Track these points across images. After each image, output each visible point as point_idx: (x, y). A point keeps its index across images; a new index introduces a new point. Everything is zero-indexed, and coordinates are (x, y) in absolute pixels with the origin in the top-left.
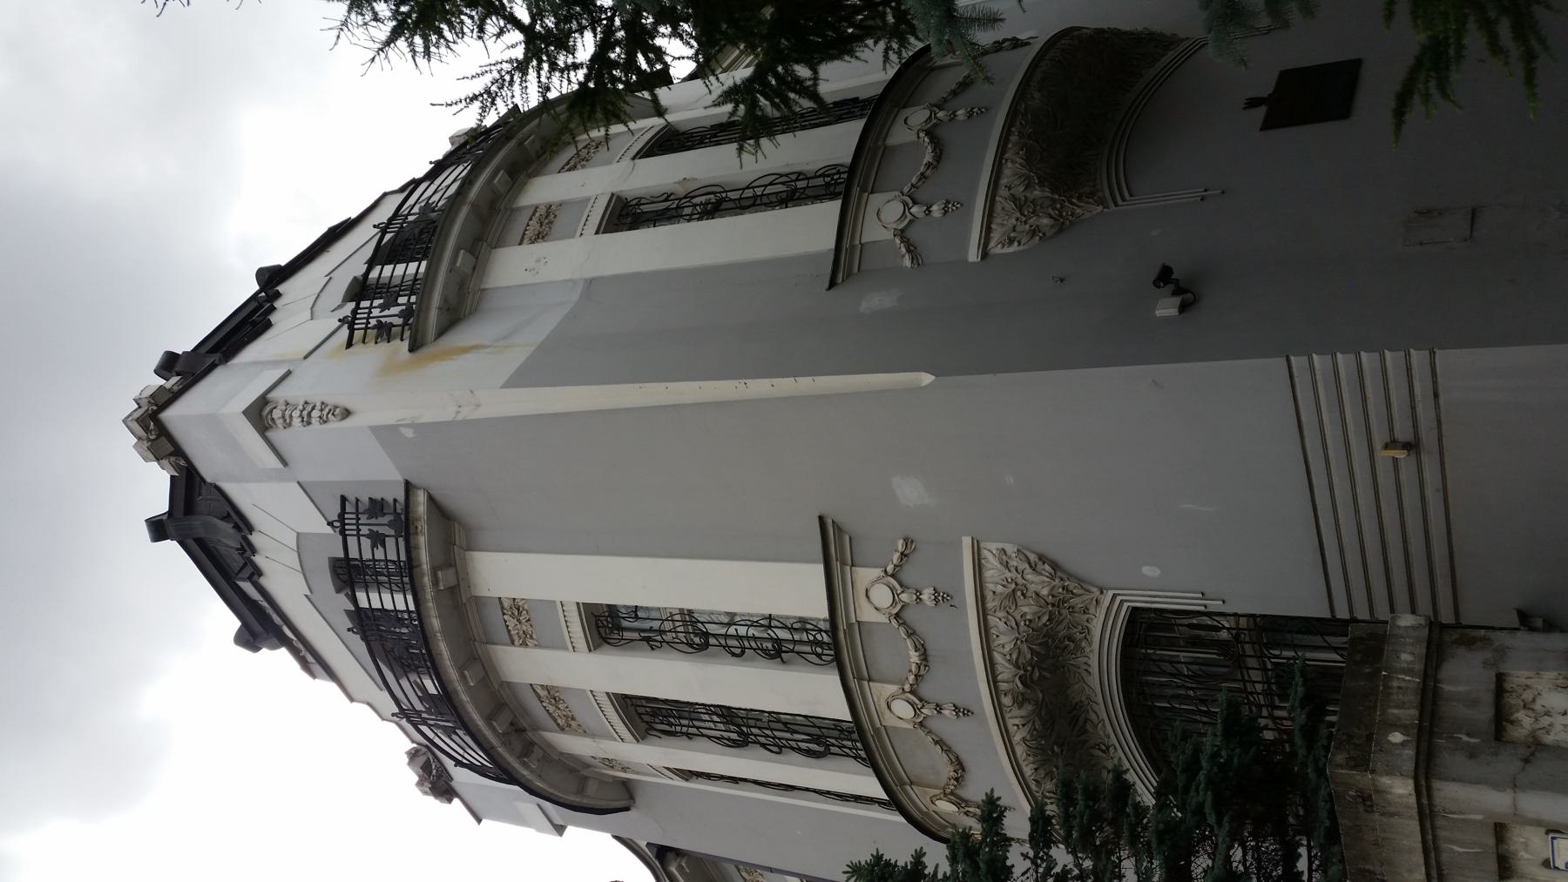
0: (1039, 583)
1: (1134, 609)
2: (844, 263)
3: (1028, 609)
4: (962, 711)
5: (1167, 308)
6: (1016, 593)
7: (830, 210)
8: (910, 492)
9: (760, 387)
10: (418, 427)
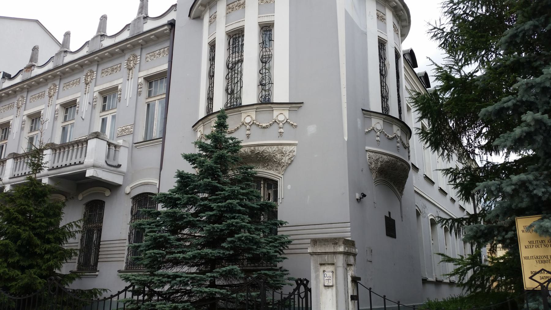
0: (285, 160)
1: (277, 182)
2: (367, 113)
3: (279, 156)
4: (248, 136)
5: (358, 196)
8: (312, 129)
9: (344, 92)
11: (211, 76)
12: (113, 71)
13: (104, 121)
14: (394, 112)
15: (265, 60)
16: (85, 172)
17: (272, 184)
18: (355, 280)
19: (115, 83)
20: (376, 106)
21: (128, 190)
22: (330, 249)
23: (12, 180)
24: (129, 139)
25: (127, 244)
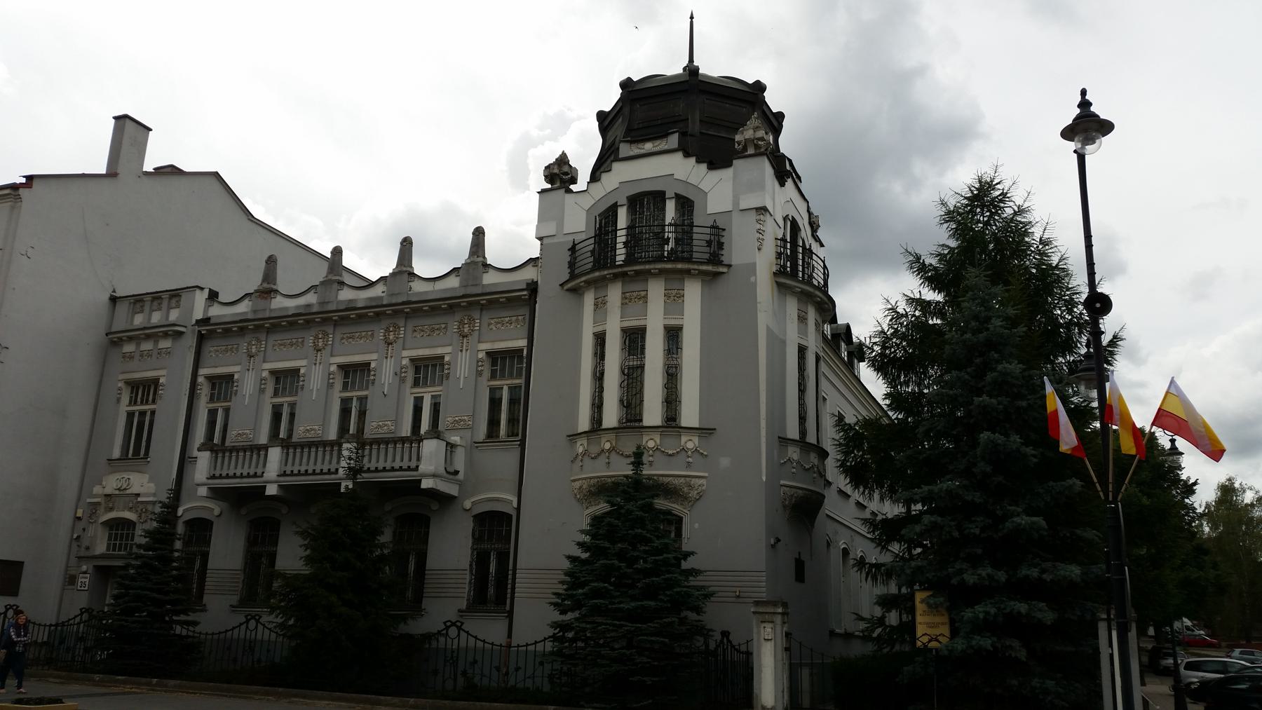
0: (694, 494)
1: (681, 519)
2: (784, 441)
5: (772, 541)
7: (797, 437)
8: (725, 462)
9: (763, 424)
10: (755, 284)
11: (599, 377)
12: (433, 330)
14: (811, 439)
18: (788, 635)
19: (439, 351)
20: (793, 432)
21: (468, 504)
23: (282, 479)
24: (468, 434)
25: (468, 577)
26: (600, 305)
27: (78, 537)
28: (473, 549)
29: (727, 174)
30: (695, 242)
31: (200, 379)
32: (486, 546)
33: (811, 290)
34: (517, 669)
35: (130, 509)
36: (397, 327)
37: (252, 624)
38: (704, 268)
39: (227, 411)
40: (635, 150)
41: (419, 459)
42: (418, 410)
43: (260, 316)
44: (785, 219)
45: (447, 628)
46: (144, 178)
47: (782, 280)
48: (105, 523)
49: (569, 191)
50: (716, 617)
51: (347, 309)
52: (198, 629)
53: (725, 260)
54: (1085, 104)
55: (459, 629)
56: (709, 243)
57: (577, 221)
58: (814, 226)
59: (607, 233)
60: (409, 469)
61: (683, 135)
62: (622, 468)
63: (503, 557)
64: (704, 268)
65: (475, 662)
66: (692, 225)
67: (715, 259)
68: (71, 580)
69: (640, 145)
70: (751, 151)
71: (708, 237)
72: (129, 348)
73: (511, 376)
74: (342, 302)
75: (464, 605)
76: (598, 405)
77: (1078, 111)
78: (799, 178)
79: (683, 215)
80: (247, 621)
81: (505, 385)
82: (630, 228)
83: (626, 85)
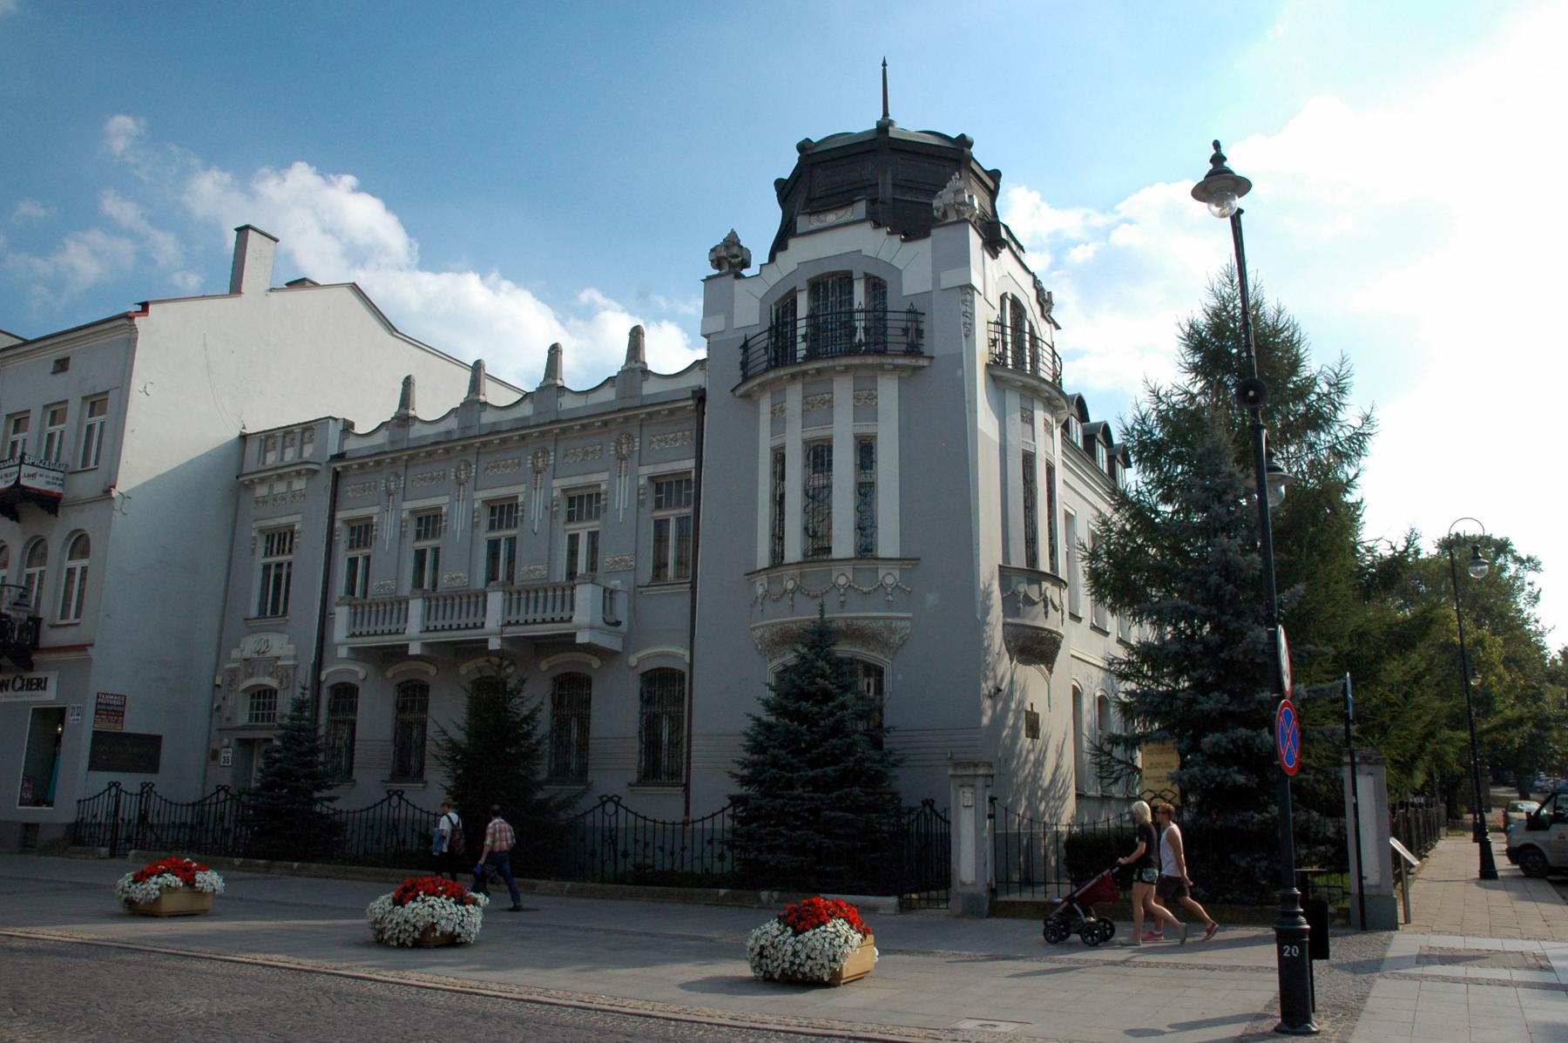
0: (896, 639)
6: (892, 631)
11: (779, 501)
12: (586, 453)
13: (574, 539)
15: (865, 491)
16: (574, 635)
17: (876, 672)
18: (992, 800)
19: (594, 478)
21: (633, 661)
22: (971, 772)
26: (778, 414)
27: (219, 707)
28: (642, 714)
29: (923, 247)
30: (890, 331)
31: (338, 524)
32: (657, 709)
33: (1036, 383)
34: (683, 849)
35: (271, 675)
36: (546, 452)
37: (395, 799)
38: (900, 361)
39: (367, 559)
40: (815, 222)
41: (572, 608)
42: (573, 553)
43: (399, 447)
44: (1003, 298)
45: (604, 803)
46: (273, 295)
47: (999, 373)
48: (244, 691)
49: (739, 276)
50: (909, 786)
51: (489, 434)
52: (336, 805)
53: (926, 350)
54: (1218, 159)
55: (617, 804)
56: (906, 331)
57: (750, 313)
58: (1045, 301)
59: (786, 324)
60: (562, 620)
61: (873, 202)
62: (805, 614)
63: (677, 722)
64: (900, 361)
65: (636, 841)
66: (885, 312)
67: (913, 350)
68: (215, 755)
69: (822, 217)
70: (952, 217)
71: (903, 325)
72: (262, 491)
73: (679, 505)
74: (480, 427)
75: (633, 777)
76: (778, 536)
77: (1210, 167)
78: (1021, 248)
79: (875, 298)
80: (390, 797)
81: (671, 514)
82: (810, 316)
83: (804, 147)
